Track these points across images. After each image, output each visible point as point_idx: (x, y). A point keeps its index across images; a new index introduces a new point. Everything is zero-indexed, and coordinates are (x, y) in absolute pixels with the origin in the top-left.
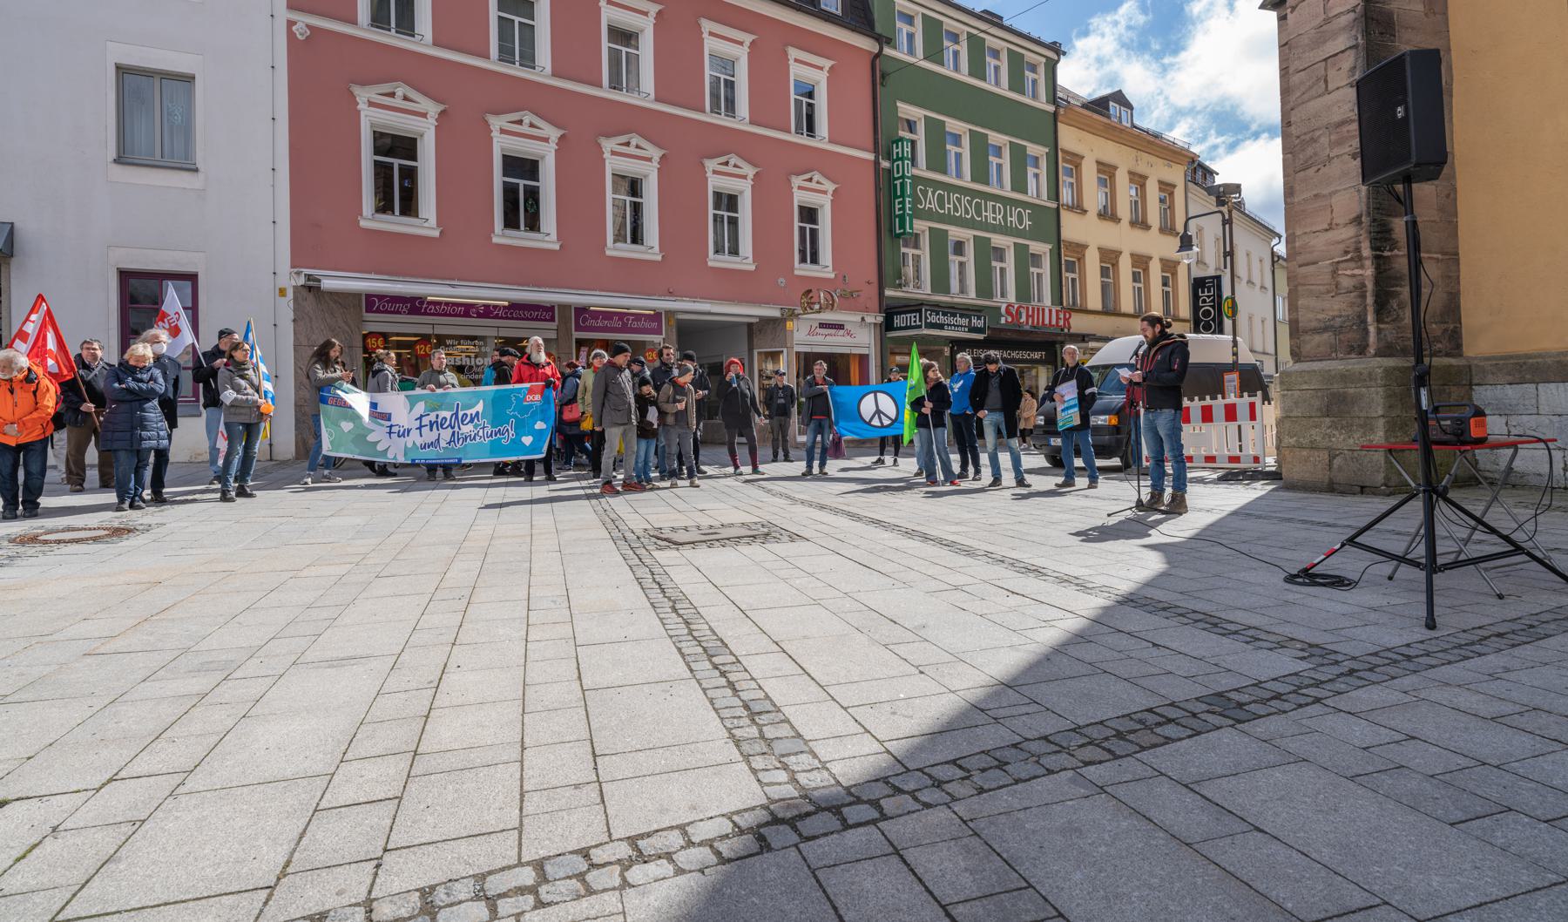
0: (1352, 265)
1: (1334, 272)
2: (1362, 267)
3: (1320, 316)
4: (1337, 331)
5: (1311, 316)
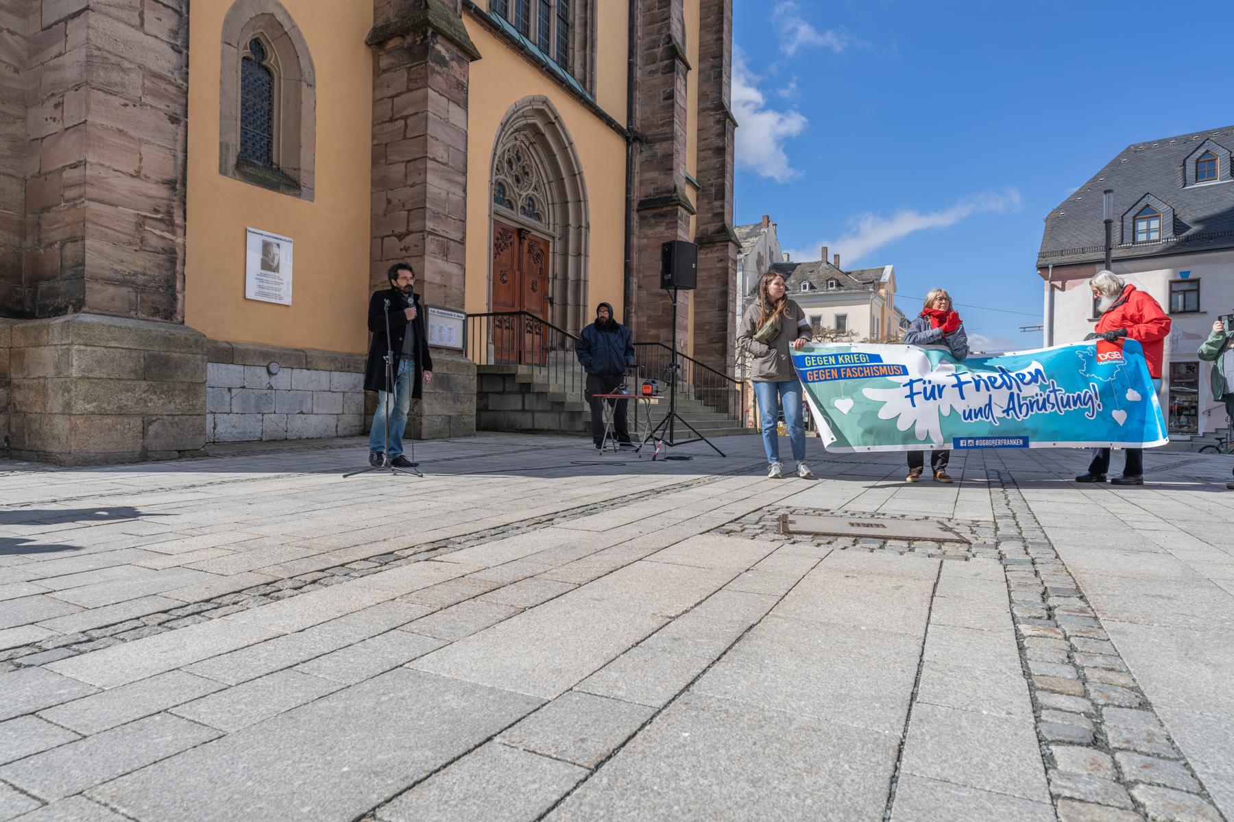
0: (162, 226)
1: (140, 224)
2: (173, 233)
3: (116, 266)
4: (141, 289)
5: (104, 262)
